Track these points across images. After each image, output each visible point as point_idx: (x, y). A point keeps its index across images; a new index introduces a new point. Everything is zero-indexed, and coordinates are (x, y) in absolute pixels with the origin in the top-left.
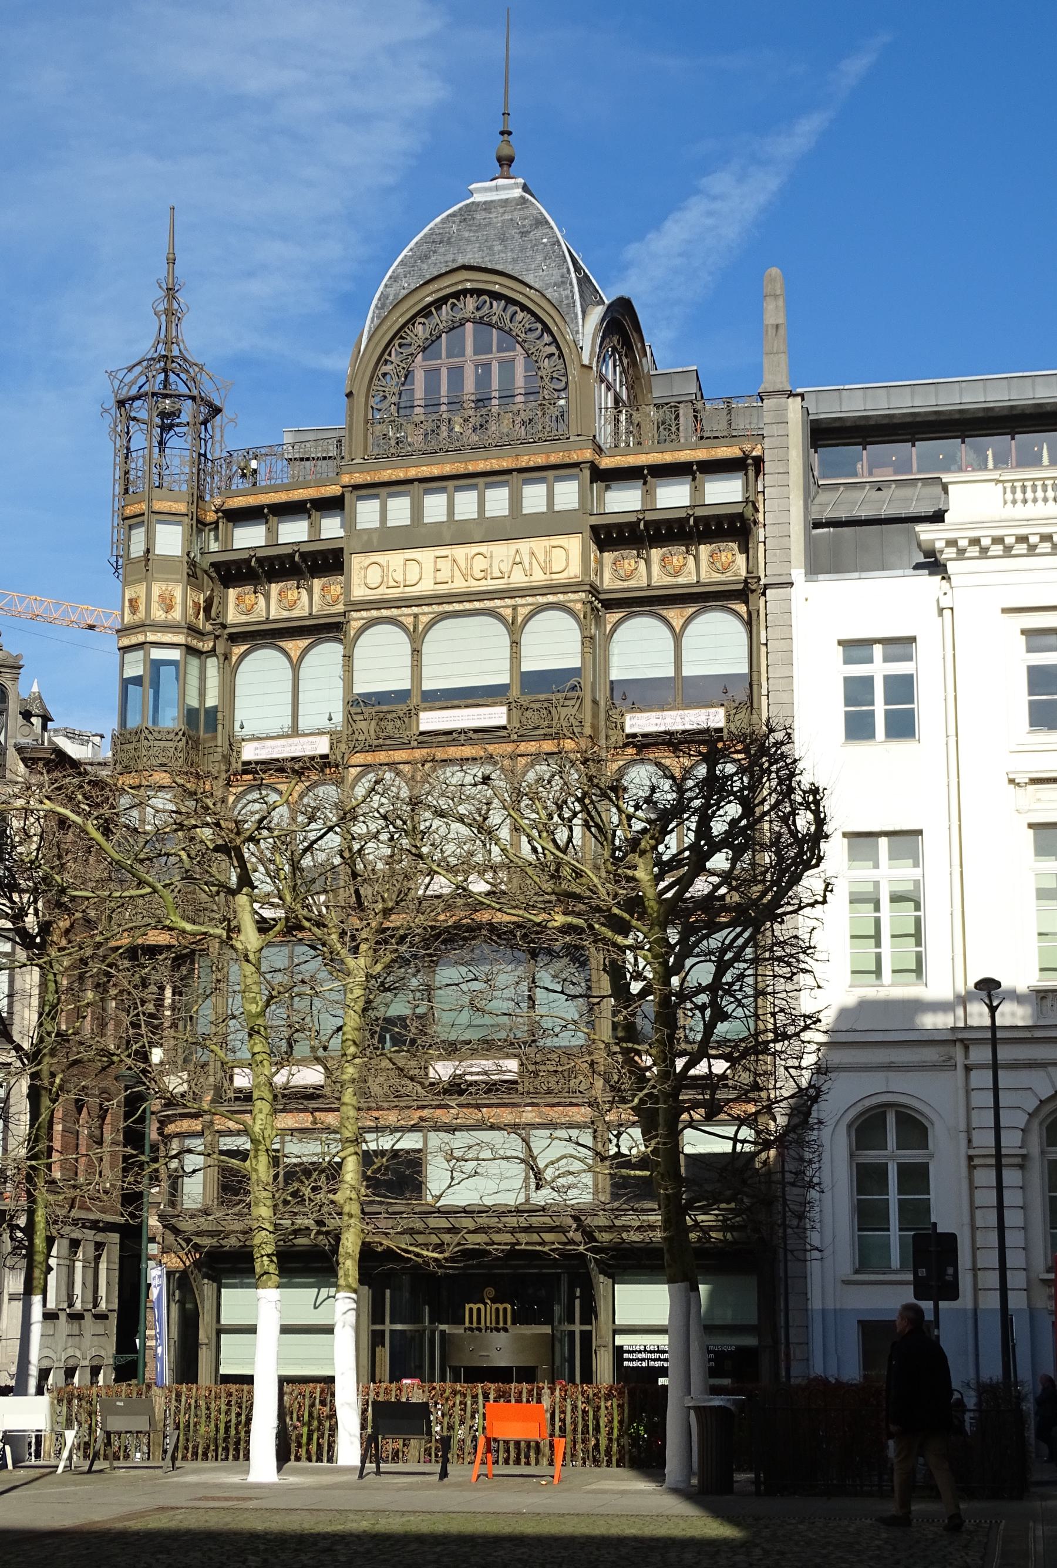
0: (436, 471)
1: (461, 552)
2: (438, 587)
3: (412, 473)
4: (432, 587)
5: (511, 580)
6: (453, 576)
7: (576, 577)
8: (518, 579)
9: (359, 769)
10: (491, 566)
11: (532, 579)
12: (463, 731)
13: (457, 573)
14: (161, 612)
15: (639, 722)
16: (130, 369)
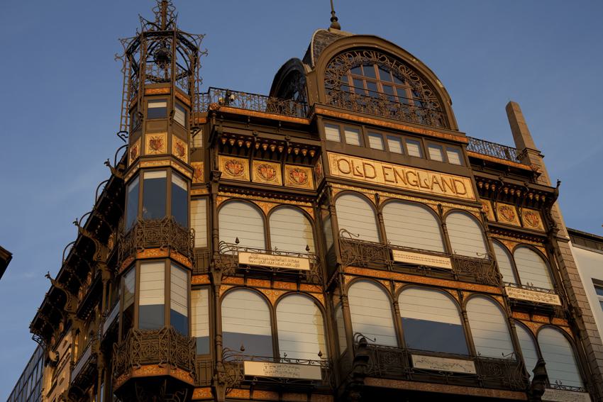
0: (376, 122)
1: (399, 169)
2: (387, 183)
3: (362, 120)
4: (384, 182)
5: (434, 191)
6: (396, 180)
7: (472, 198)
8: (437, 190)
9: (352, 277)
10: (420, 180)
11: (446, 193)
12: (424, 267)
13: (398, 177)
14: (177, 154)
15: (514, 293)
16: (149, 23)
